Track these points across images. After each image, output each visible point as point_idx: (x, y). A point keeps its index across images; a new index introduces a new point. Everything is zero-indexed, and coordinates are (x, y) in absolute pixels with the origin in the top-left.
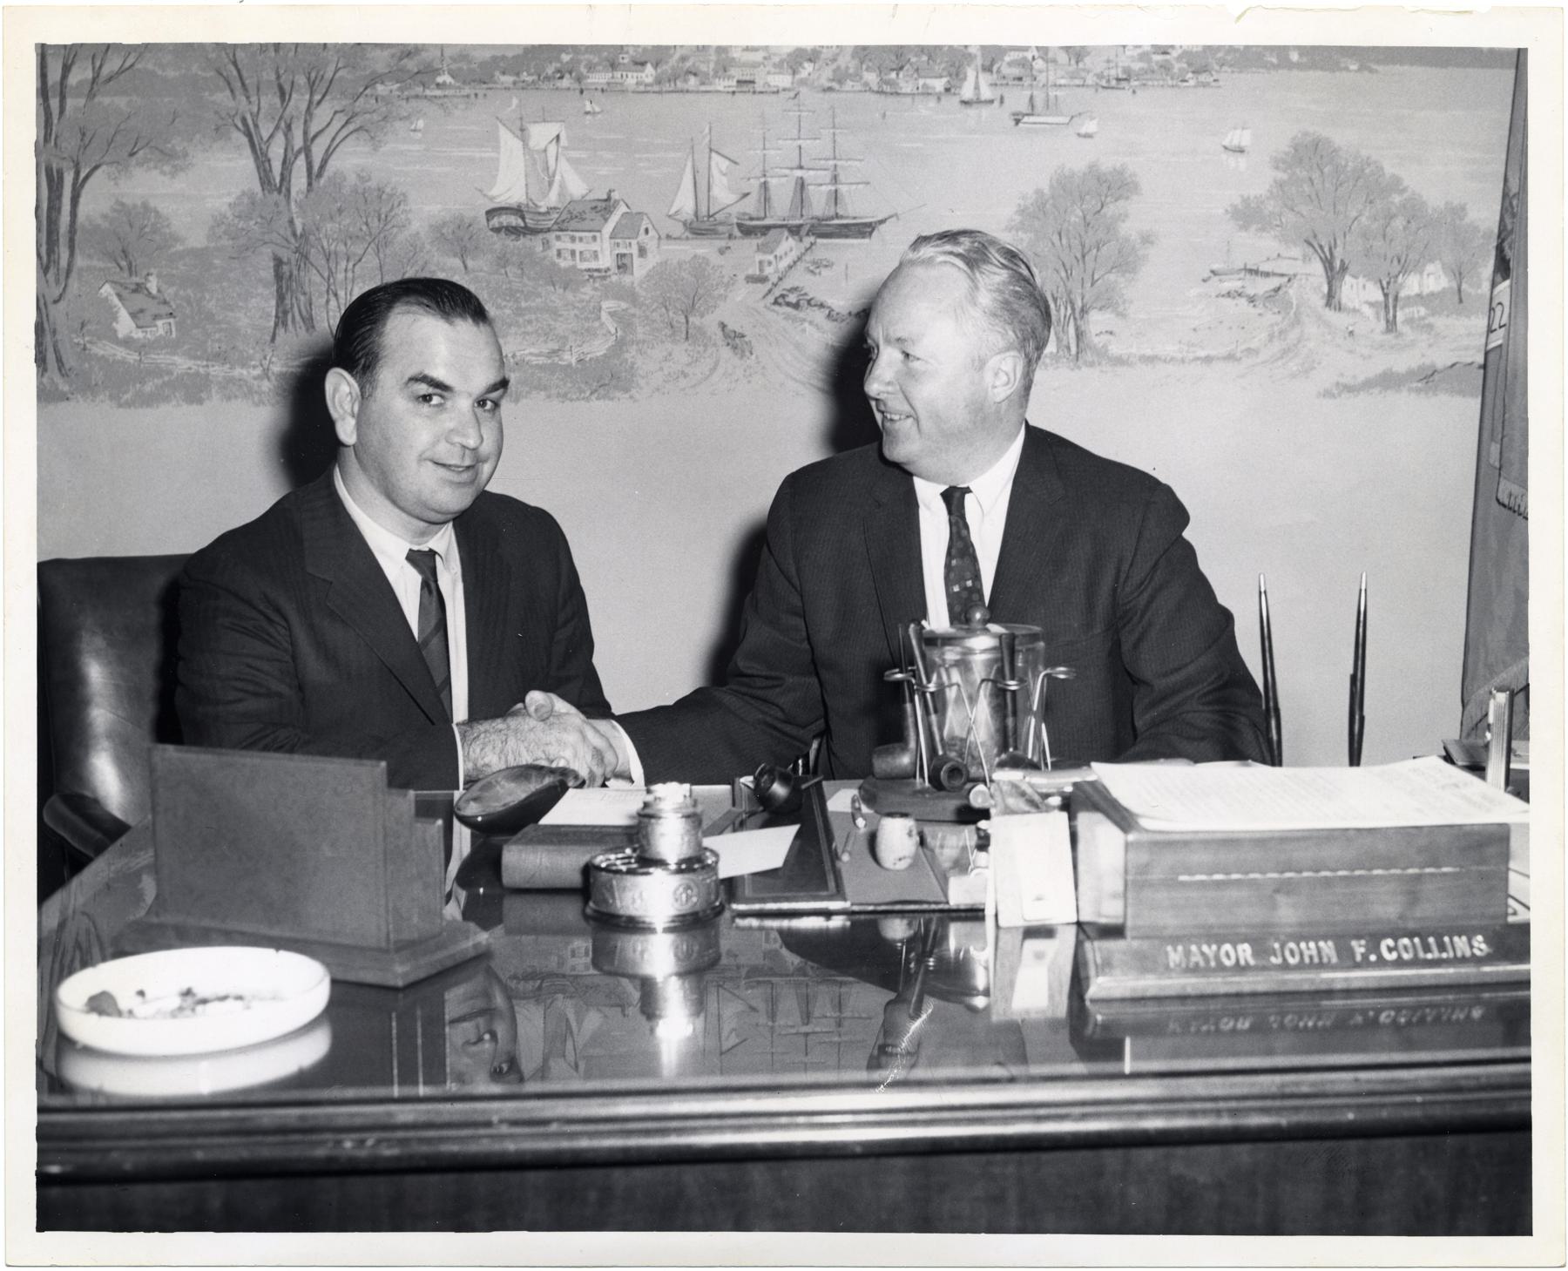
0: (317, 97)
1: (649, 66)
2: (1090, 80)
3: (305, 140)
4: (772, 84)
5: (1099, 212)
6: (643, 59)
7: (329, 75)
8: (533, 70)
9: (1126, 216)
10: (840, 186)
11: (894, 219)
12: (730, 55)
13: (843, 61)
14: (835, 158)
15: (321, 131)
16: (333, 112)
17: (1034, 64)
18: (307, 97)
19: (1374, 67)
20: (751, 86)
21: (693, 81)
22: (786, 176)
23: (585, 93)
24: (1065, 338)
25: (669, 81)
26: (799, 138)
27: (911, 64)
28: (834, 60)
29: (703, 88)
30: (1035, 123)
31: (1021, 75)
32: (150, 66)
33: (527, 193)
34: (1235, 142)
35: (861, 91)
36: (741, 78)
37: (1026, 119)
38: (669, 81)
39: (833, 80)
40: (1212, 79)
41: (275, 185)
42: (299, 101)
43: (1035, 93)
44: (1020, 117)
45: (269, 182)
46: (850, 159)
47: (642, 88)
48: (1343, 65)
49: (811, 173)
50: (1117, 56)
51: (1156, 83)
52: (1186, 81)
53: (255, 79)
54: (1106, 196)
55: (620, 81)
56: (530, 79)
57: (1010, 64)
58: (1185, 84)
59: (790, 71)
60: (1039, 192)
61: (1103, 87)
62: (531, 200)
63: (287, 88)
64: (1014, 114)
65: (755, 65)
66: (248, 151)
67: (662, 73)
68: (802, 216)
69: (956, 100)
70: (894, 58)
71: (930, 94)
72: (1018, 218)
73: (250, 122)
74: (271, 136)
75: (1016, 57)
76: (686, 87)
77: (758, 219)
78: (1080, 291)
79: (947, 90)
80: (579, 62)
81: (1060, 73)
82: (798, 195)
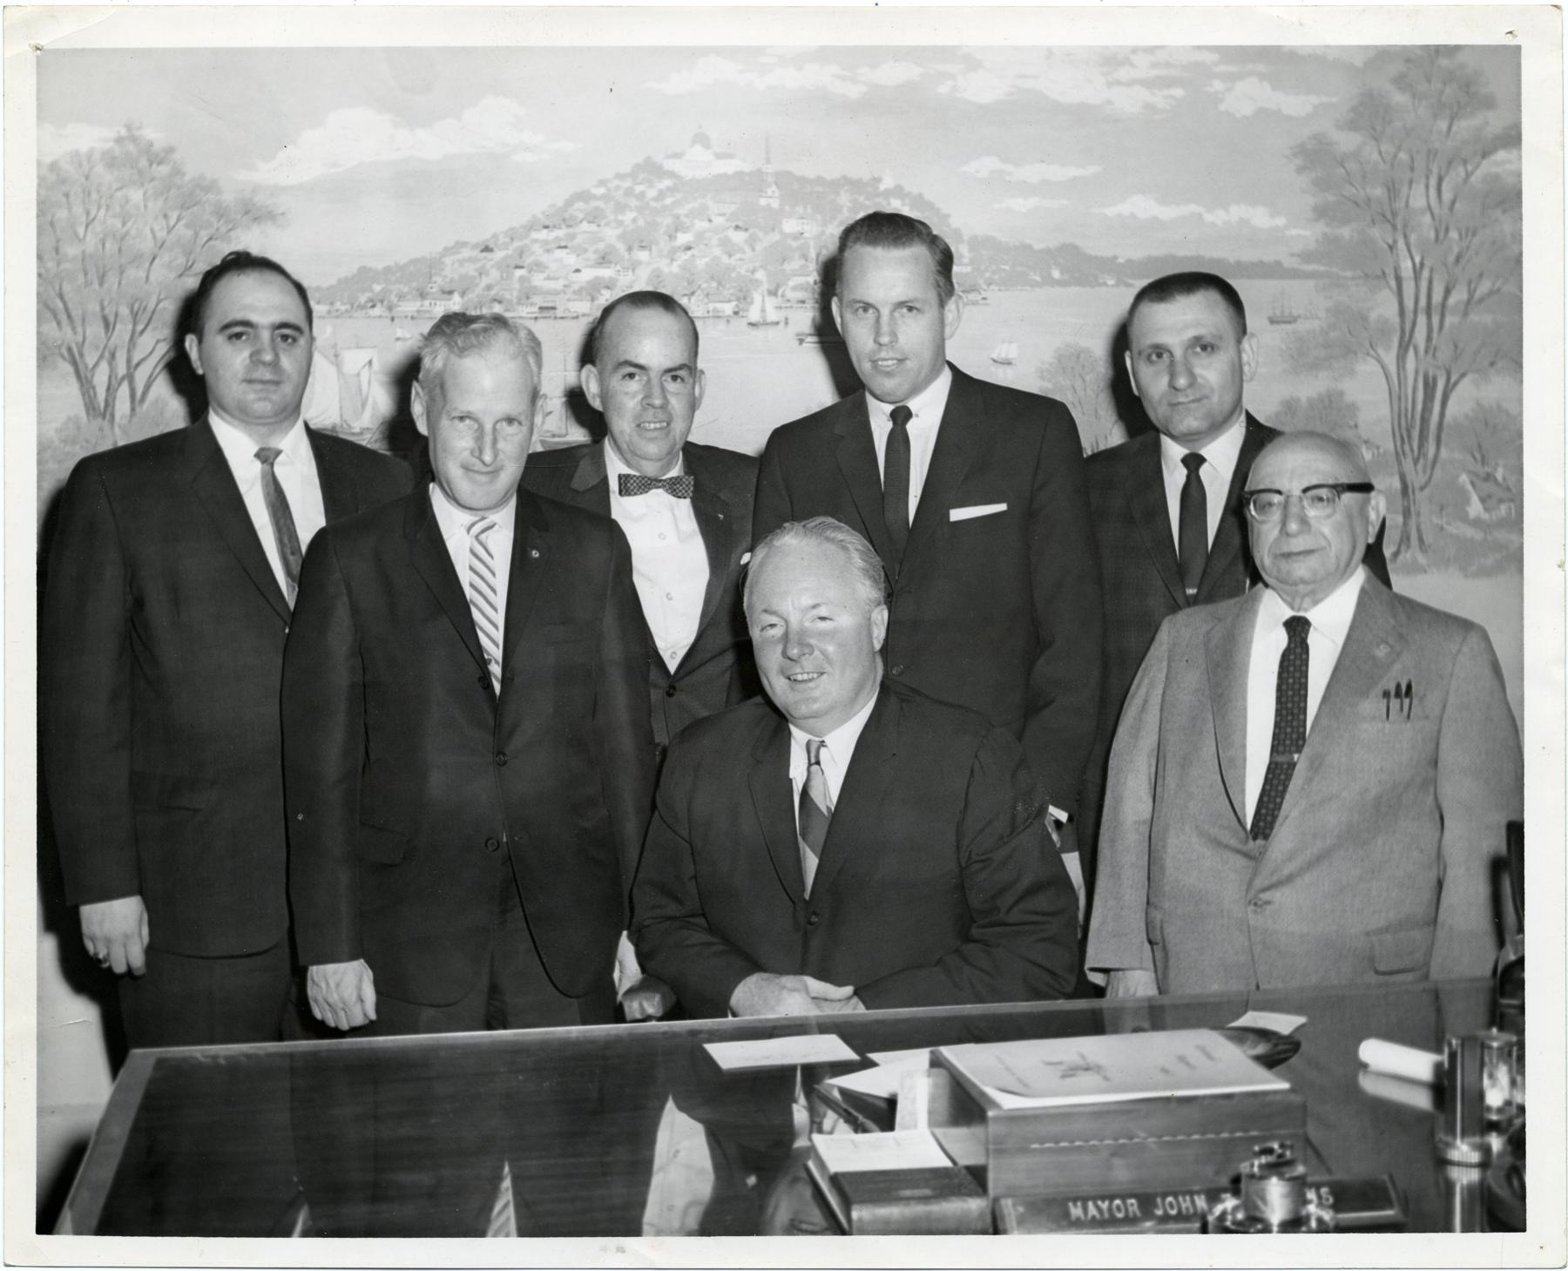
0: (140, 327)
3: (129, 367)
4: (572, 310)
6: (453, 289)
7: (151, 306)
8: (345, 301)
15: (144, 360)
16: (155, 341)
18: (130, 327)
19: (1130, 281)
20: (552, 312)
23: (396, 320)
27: (702, 290)
33: (341, 416)
34: (1003, 355)
40: (981, 297)
41: (100, 410)
42: (122, 331)
44: (804, 337)
45: (94, 409)
48: (1101, 281)
53: (80, 312)
55: (430, 309)
56: (343, 308)
57: (794, 289)
59: (590, 298)
62: (345, 421)
63: (111, 319)
64: (798, 335)
65: (556, 293)
66: (73, 379)
69: (744, 322)
70: (686, 284)
71: (719, 317)
73: (75, 351)
74: (96, 365)
75: (799, 282)
77: (560, 436)
79: (736, 313)
80: (391, 292)
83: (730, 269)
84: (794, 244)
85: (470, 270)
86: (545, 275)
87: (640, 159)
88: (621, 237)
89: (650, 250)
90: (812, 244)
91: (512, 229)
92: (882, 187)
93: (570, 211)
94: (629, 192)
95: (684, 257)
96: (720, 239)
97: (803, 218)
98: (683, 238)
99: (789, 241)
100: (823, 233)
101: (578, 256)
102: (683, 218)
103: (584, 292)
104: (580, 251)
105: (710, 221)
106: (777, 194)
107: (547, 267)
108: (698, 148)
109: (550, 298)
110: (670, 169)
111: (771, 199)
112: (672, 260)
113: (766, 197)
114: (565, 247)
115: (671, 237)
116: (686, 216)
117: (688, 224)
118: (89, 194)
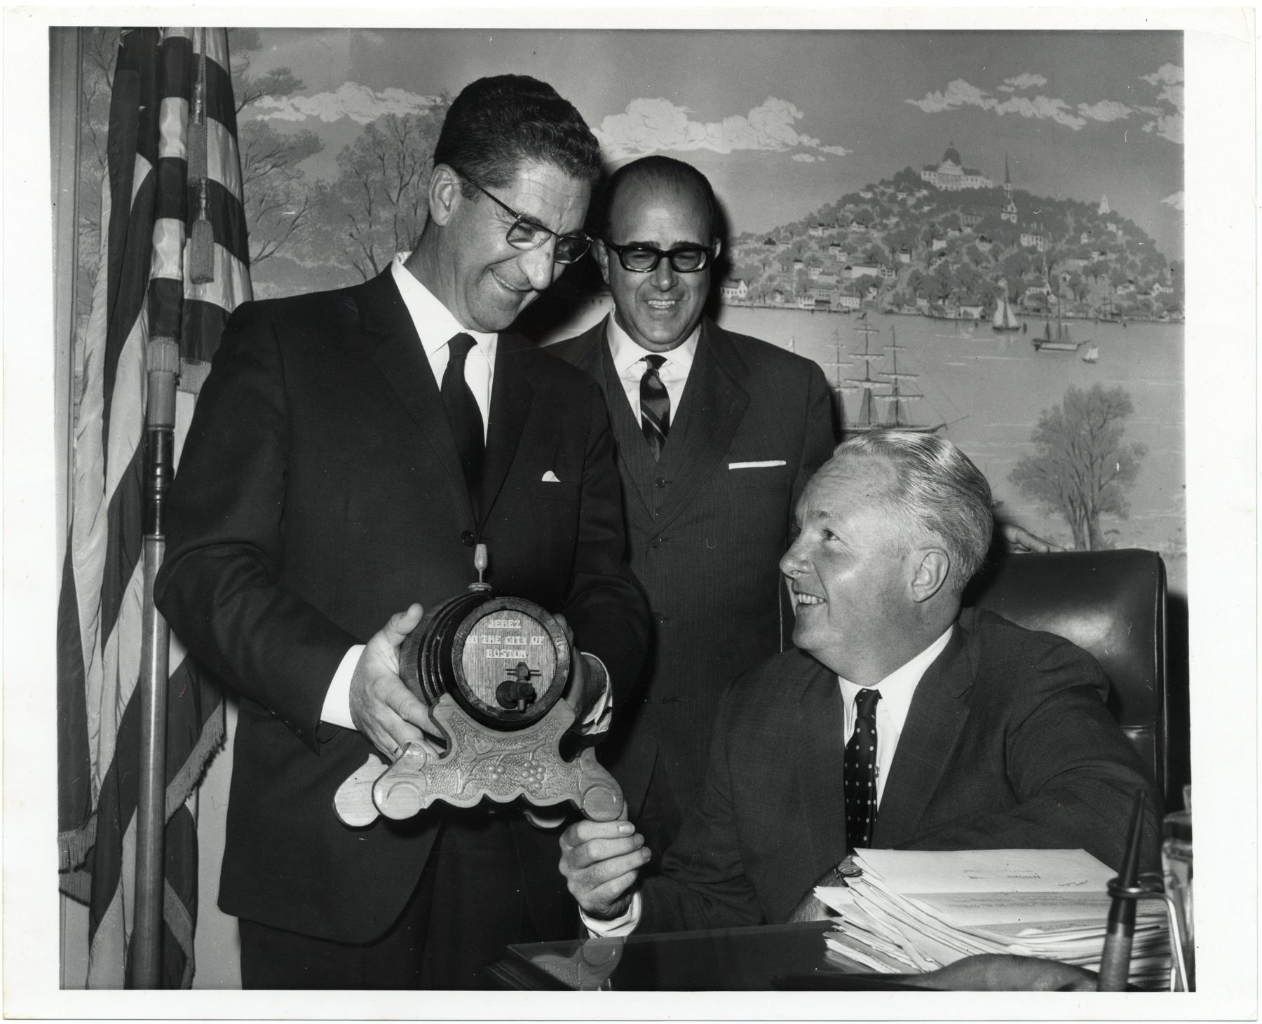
1: (742, 283)
2: (1091, 314)
4: (844, 305)
5: (1102, 427)
9: (1123, 430)
10: (899, 398)
11: (943, 429)
12: (809, 277)
13: (899, 289)
14: (895, 374)
17: (1049, 297)
20: (827, 305)
21: (779, 298)
22: (856, 387)
24: (1081, 536)
25: (760, 297)
26: (866, 354)
28: (894, 286)
29: (787, 305)
30: (1050, 349)
31: (1038, 307)
32: (289, 256)
35: (915, 315)
36: (819, 298)
37: (1044, 345)
38: (760, 297)
39: (892, 304)
43: (1051, 323)
46: (907, 375)
47: (736, 303)
49: (878, 385)
50: (1110, 294)
51: (1140, 319)
52: (1161, 317)
54: (1107, 414)
57: (1032, 297)
58: (1162, 320)
59: (859, 295)
60: (1056, 408)
61: (1102, 321)
64: (1035, 340)
65: (829, 287)
67: (753, 289)
68: (870, 423)
69: (989, 327)
70: (941, 287)
72: (1041, 431)
75: (1035, 292)
76: (773, 304)
78: (1090, 494)
79: (983, 317)
81: (1069, 307)
82: (867, 401)
83: (977, 276)
84: (1030, 257)
85: (755, 260)
86: (821, 270)
87: (903, 171)
88: (884, 240)
89: (911, 254)
90: (1045, 259)
91: (791, 224)
92: (1100, 212)
93: (842, 212)
94: (892, 199)
95: (939, 262)
96: (969, 248)
97: (1035, 234)
98: (938, 245)
99: (1026, 254)
100: (1053, 249)
101: (849, 254)
102: (937, 226)
103: (854, 289)
104: (850, 250)
105: (960, 230)
106: (1015, 211)
107: (822, 263)
108: (949, 162)
109: (825, 292)
110: (927, 180)
111: (1010, 214)
112: (930, 264)
113: (1006, 212)
114: (838, 245)
115: (929, 244)
116: (940, 224)
117: (942, 232)
118: (404, 158)
